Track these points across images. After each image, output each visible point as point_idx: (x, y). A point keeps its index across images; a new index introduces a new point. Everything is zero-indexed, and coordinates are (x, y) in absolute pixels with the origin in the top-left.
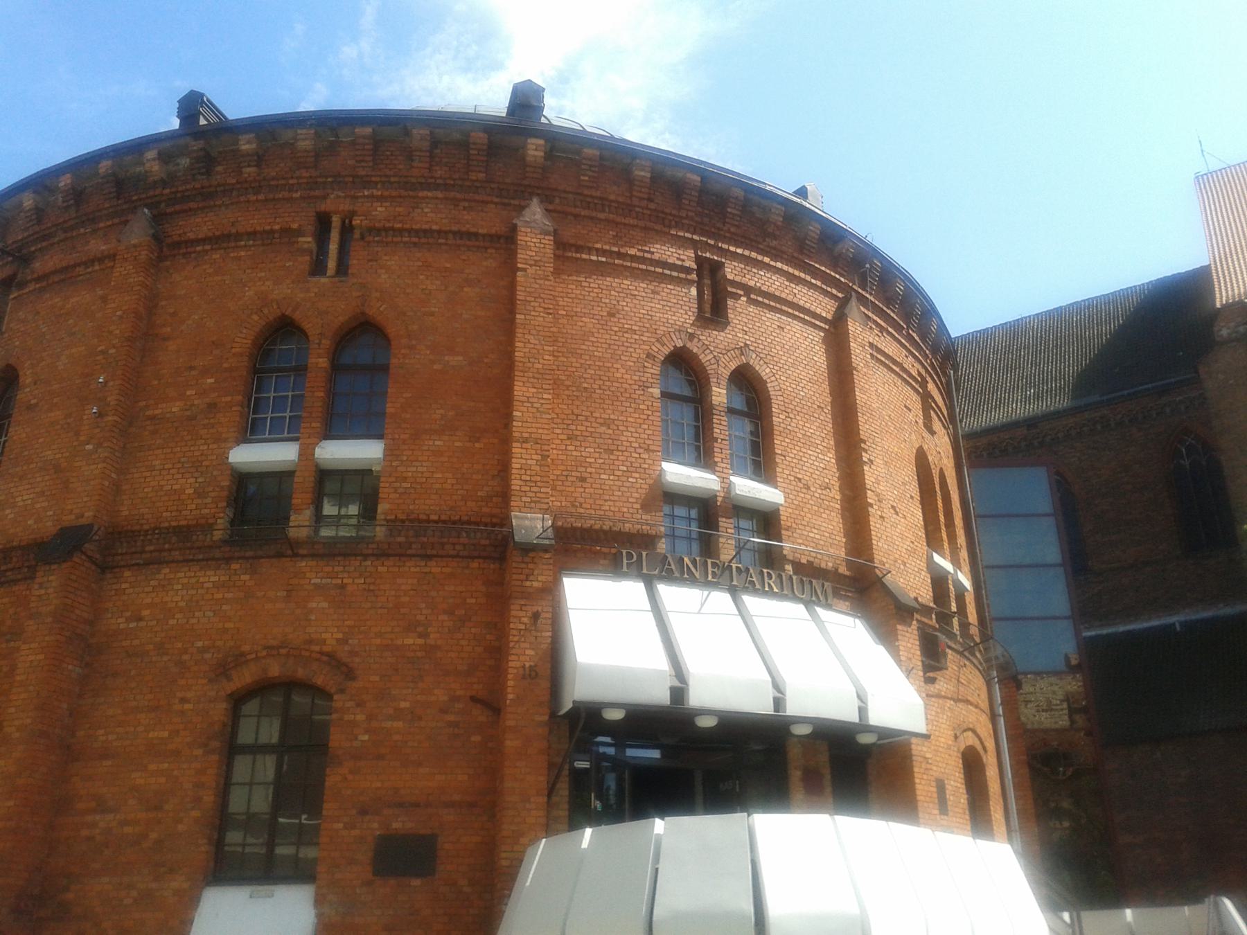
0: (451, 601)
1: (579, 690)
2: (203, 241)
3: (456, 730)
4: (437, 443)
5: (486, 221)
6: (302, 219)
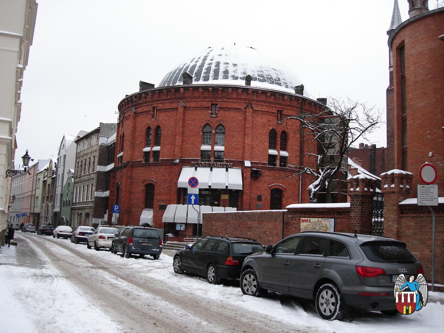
1: (179, 186)
2: (139, 113)
5: (174, 106)
6: (150, 108)
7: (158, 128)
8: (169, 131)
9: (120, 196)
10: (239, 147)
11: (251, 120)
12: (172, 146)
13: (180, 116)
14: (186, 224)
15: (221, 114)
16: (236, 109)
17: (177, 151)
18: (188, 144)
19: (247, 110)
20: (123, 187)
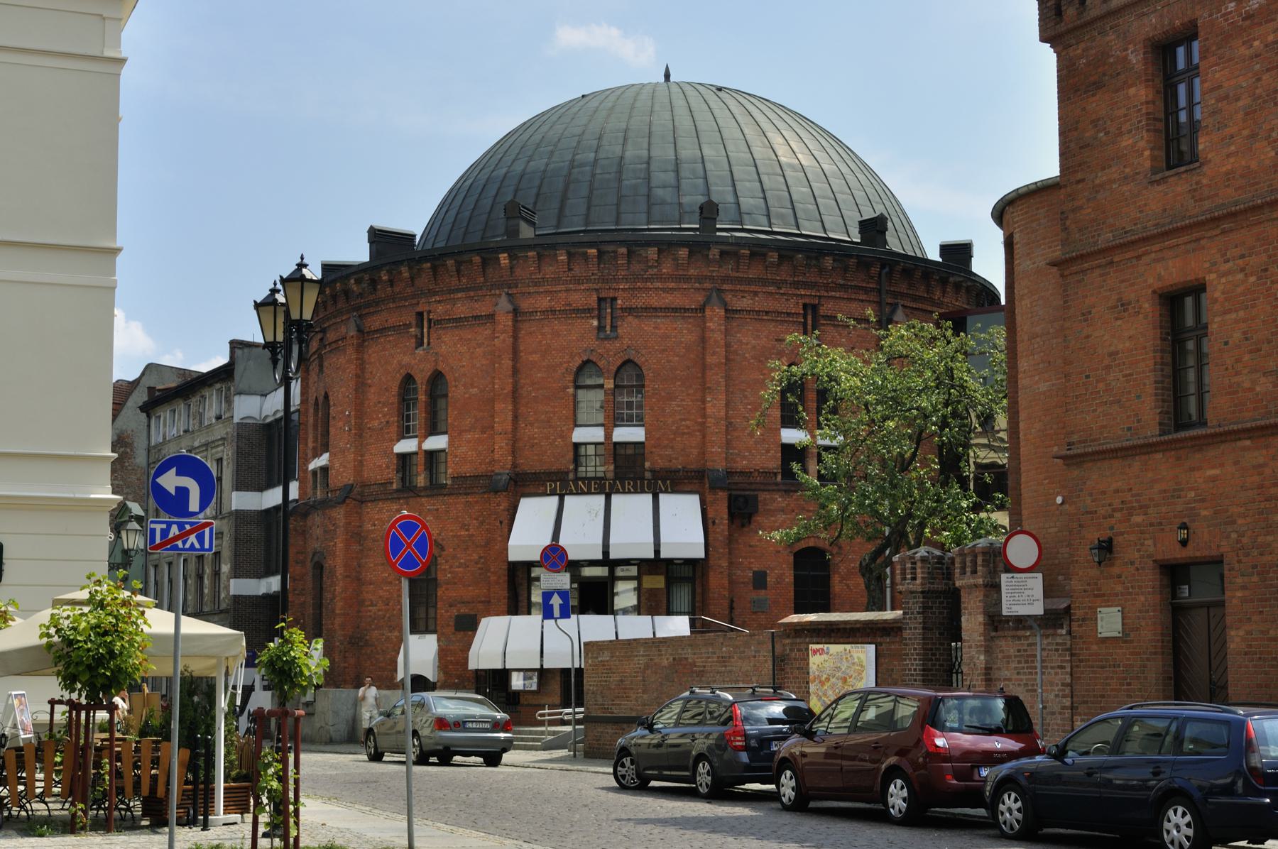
5: (482, 308)
6: (410, 318)
7: (437, 378)
8: (472, 386)
9: (327, 595)
10: (688, 427)
11: (722, 342)
12: (483, 432)
13: (503, 340)
14: (543, 673)
15: (628, 326)
16: (675, 310)
17: (501, 448)
18: (532, 424)
19: (708, 312)
20: (337, 564)
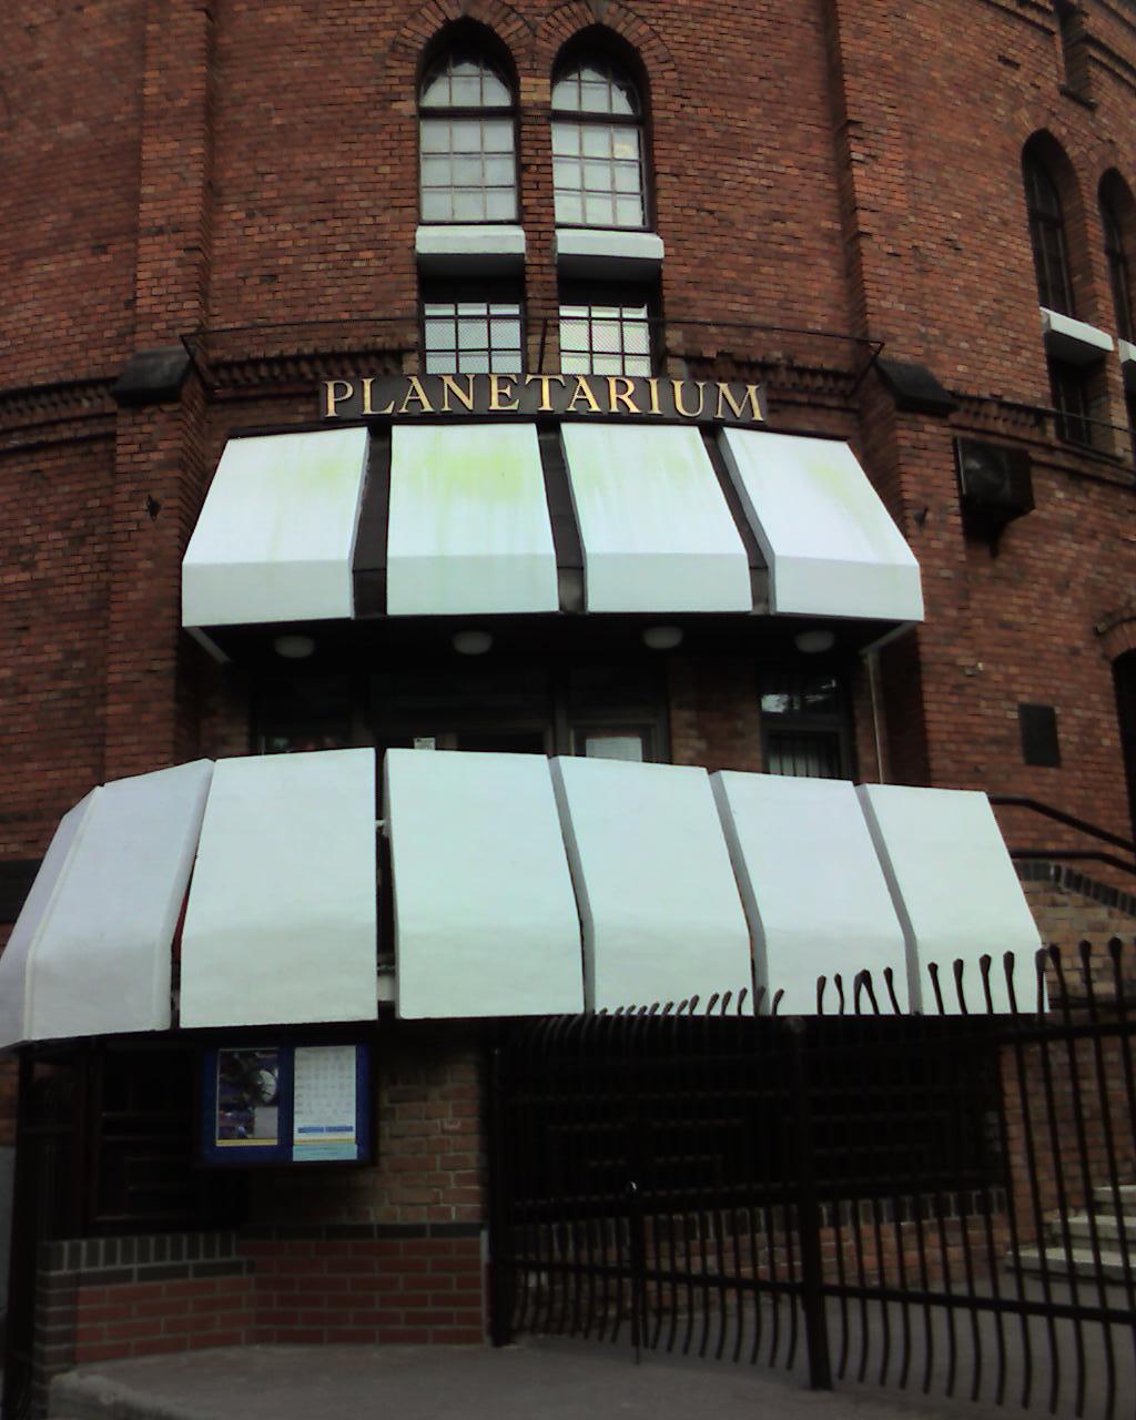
0: (65, 508)
1: (202, 608)
3: (76, 703)
4: (47, 268)
8: (67, 116)
17: (160, 276)
